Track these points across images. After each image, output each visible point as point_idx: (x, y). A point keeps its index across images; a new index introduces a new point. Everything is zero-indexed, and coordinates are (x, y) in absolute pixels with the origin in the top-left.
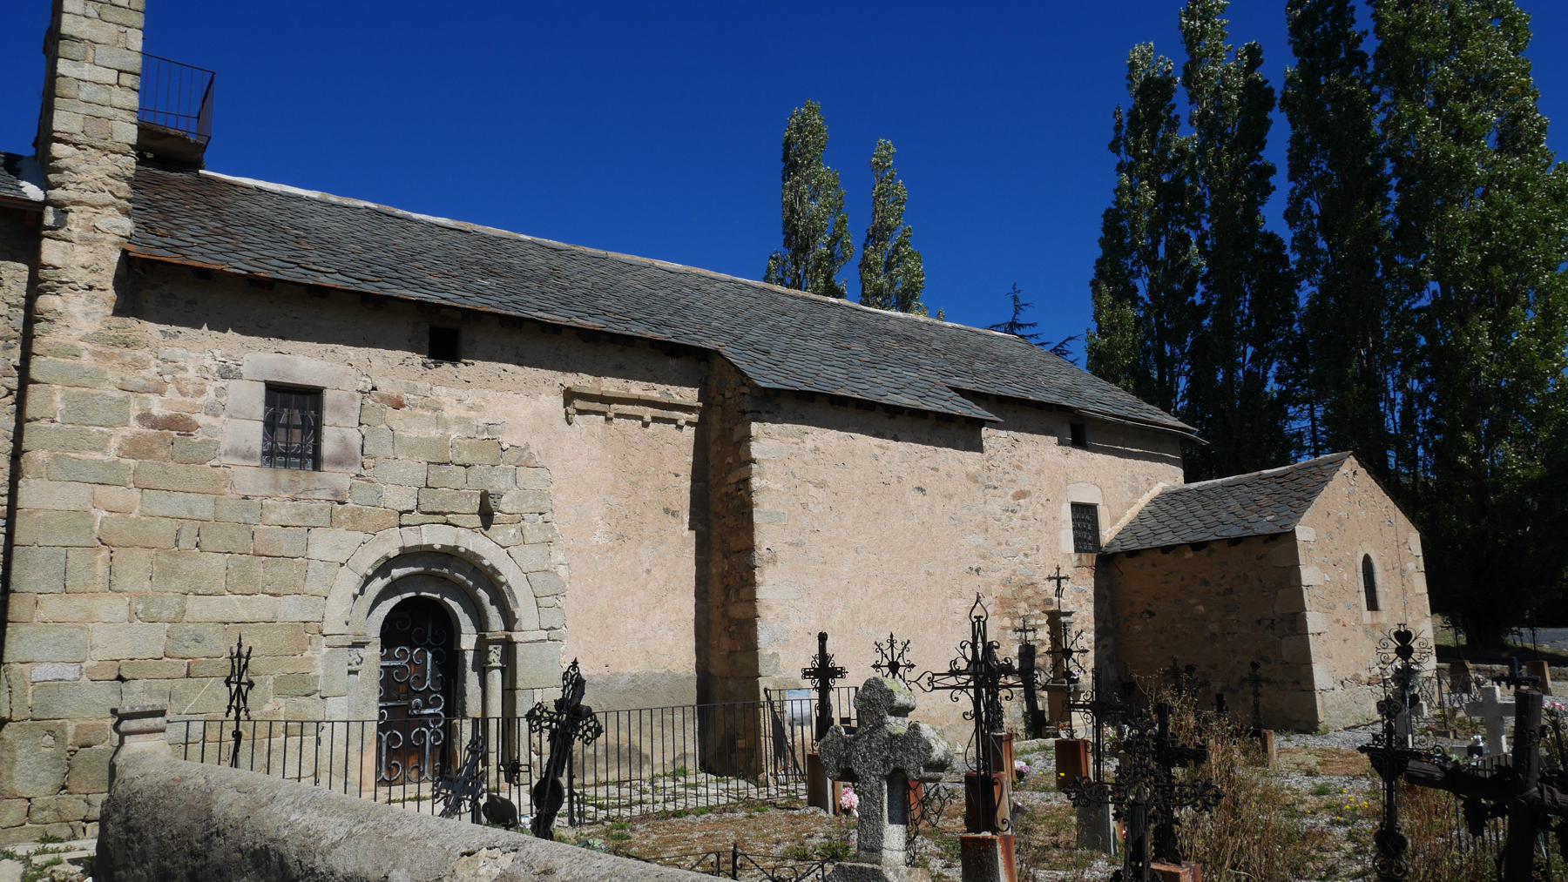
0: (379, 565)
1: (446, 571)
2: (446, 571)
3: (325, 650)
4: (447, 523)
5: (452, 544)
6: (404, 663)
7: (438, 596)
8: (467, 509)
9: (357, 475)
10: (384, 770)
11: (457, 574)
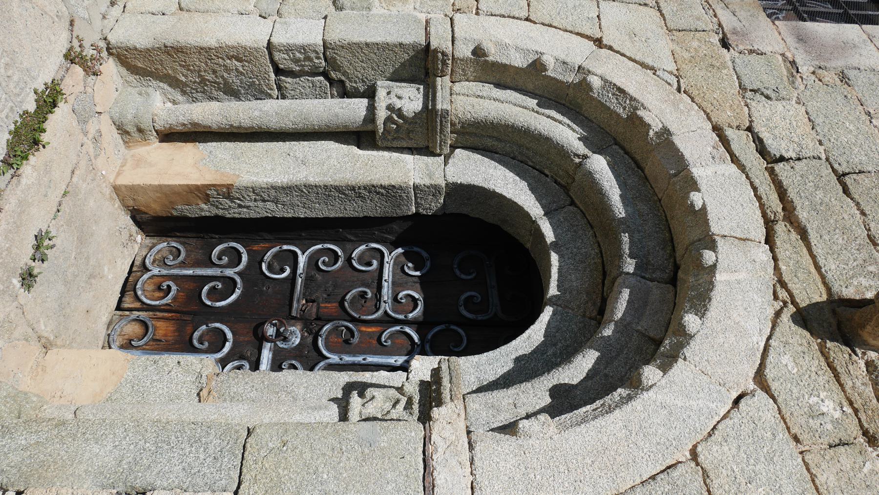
0: (613, 103)
1: (630, 266)
2: (630, 266)
3: (423, 17)
4: (769, 224)
5: (715, 228)
6: (386, 306)
7: (553, 290)
8: (830, 266)
9: (793, 63)
10: (164, 272)
11: (626, 294)
